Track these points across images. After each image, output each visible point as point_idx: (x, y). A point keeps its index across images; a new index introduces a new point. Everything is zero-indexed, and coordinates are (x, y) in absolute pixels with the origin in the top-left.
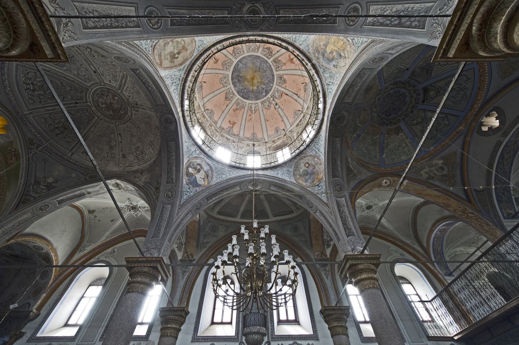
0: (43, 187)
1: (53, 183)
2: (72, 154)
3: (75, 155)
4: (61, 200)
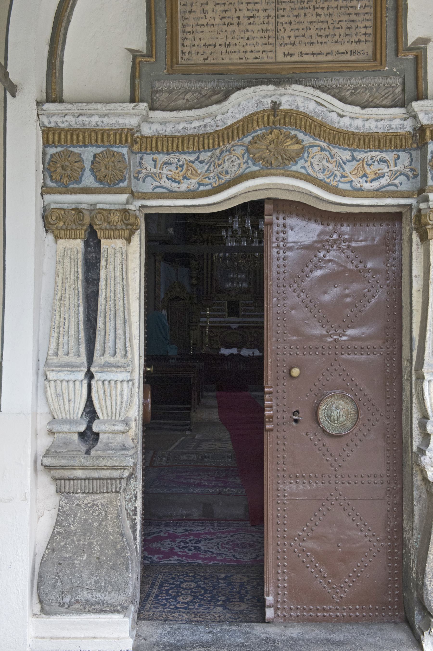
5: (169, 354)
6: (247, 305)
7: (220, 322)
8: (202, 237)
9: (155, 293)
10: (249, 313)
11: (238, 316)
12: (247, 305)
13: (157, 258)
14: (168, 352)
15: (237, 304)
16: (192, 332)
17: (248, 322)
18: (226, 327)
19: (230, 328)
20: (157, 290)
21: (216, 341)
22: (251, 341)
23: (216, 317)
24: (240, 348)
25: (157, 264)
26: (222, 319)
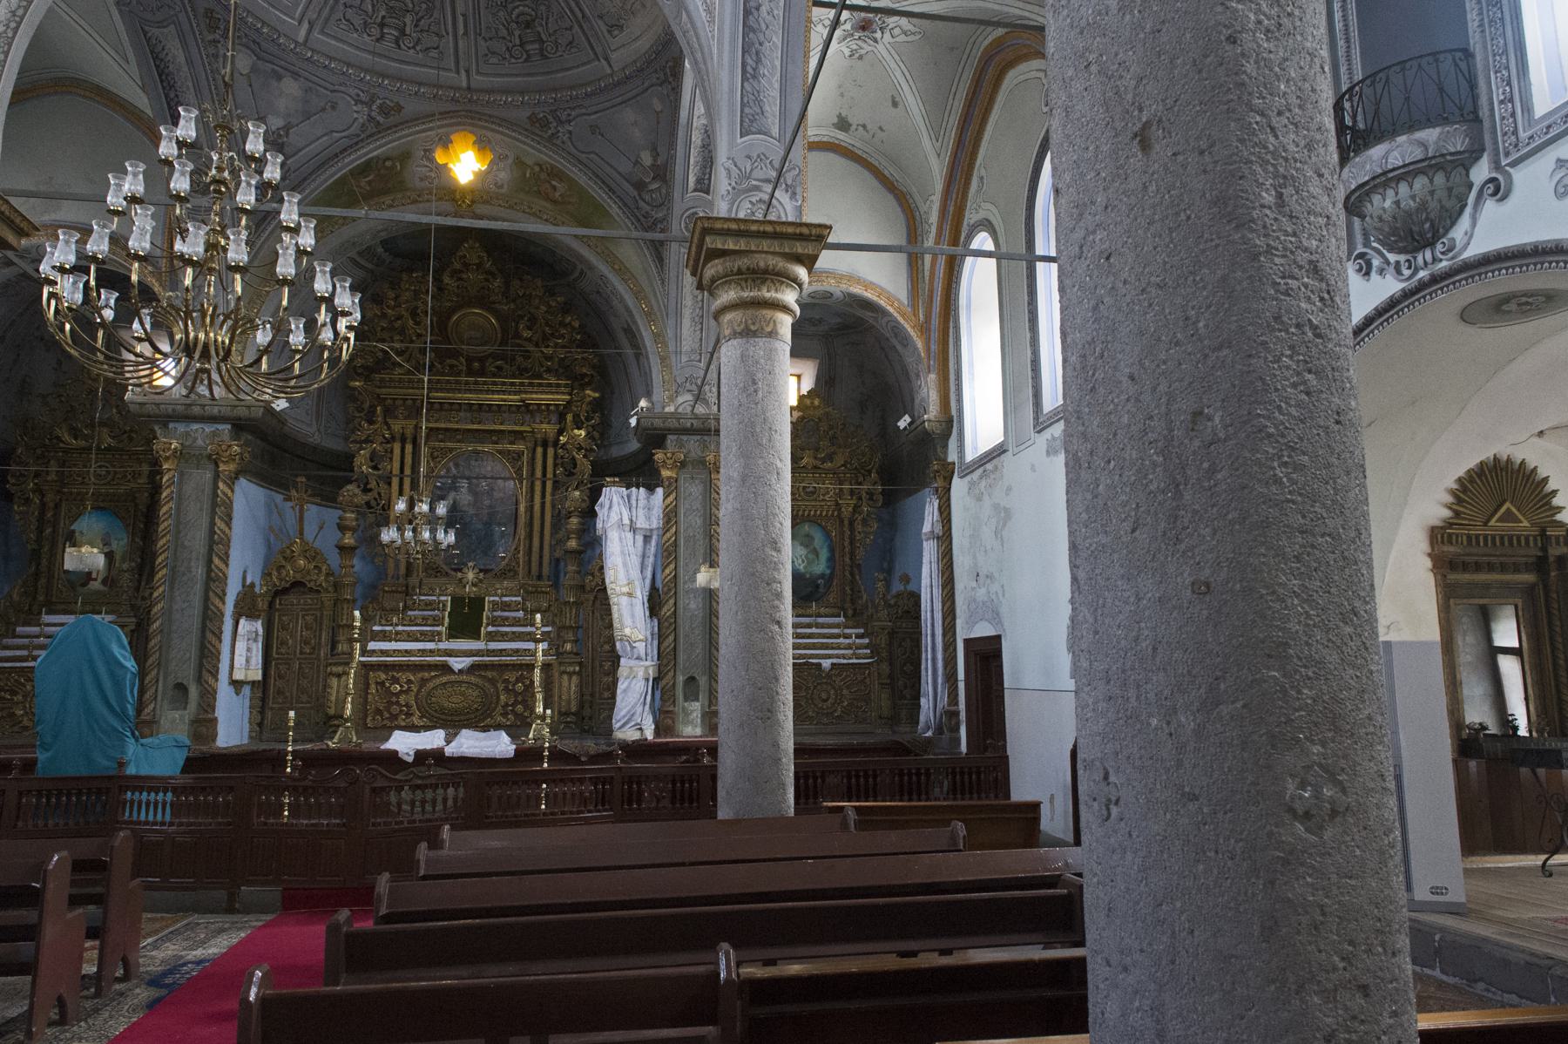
0: (654, 186)
2: (606, 59)
3: (613, 56)
4: (699, 181)
5: (131, 770)
6: (506, 607)
7: (423, 652)
8: (389, 428)
9: (209, 570)
11: (476, 635)
12: (506, 607)
13: (222, 467)
14: (121, 765)
16: (334, 682)
17: (501, 652)
19: (446, 668)
20: (216, 561)
21: (407, 705)
22: (507, 705)
23: (417, 640)
25: (221, 485)
26: (430, 646)
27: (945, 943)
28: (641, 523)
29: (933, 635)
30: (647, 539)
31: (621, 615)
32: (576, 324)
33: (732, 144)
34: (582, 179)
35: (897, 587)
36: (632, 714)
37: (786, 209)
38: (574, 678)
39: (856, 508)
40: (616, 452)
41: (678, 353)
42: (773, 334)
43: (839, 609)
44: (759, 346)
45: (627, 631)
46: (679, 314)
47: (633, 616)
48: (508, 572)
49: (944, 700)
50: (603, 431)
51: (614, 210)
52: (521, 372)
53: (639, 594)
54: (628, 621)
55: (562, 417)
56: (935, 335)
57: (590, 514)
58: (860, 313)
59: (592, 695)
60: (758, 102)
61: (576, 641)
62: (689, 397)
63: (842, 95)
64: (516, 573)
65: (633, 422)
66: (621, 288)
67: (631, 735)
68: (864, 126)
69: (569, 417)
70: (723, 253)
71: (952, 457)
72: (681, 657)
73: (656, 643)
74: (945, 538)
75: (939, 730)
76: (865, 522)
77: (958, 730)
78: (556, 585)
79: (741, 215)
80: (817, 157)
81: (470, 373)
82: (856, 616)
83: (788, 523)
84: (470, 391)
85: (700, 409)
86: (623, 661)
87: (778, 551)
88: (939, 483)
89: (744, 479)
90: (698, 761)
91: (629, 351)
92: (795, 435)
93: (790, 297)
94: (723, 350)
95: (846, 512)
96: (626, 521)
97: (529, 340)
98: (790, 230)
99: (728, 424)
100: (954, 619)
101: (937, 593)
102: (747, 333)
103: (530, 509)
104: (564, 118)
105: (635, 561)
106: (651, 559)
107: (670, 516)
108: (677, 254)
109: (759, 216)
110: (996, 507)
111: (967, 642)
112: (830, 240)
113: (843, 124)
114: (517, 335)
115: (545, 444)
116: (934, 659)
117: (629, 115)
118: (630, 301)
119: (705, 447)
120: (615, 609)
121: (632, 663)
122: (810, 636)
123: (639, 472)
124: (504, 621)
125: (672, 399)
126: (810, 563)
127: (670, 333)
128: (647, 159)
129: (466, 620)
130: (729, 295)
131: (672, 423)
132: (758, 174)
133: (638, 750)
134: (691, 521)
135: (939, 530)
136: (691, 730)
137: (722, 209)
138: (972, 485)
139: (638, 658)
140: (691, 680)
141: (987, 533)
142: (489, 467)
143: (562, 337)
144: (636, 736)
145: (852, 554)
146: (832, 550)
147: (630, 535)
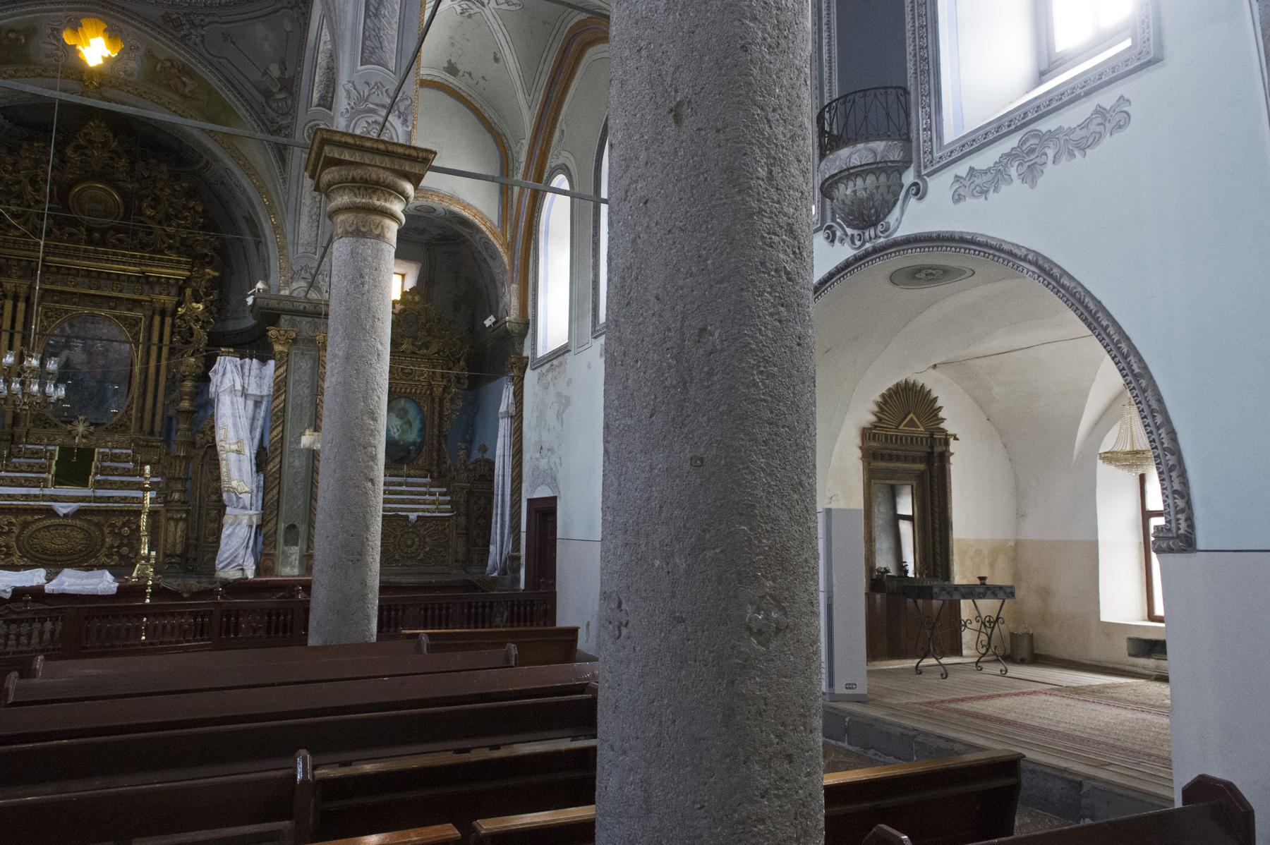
0: (281, 96)
1: (283, 73)
4: (322, 98)
6: (115, 458)
10: (117, 478)
12: (115, 458)
15: (86, 455)
17: (108, 499)
18: (40, 510)
22: (112, 547)
24: (54, 564)
27: (344, 756)
28: (253, 390)
29: (503, 495)
30: (257, 404)
31: (229, 471)
32: (200, 209)
33: (353, 67)
34: (213, 81)
35: (476, 455)
36: (236, 555)
37: (397, 132)
38: (181, 525)
39: (446, 389)
40: (233, 326)
41: (295, 244)
42: (381, 237)
43: (428, 471)
44: (368, 246)
45: (234, 484)
46: (297, 212)
47: (240, 470)
48: (121, 427)
49: (508, 547)
50: (221, 304)
51: (242, 112)
52: (143, 247)
53: (247, 451)
54: (235, 474)
55: (181, 290)
56: (519, 253)
57: (204, 379)
58: (458, 228)
59: (197, 539)
60: (378, 37)
61: (184, 491)
62: (303, 284)
63: (453, 44)
64: (128, 428)
65: (250, 300)
66: (245, 182)
67: (232, 574)
68: (470, 74)
69: (188, 291)
70: (339, 162)
71: (527, 352)
72: (284, 507)
73: (261, 495)
74: (517, 418)
75: (504, 572)
76: (452, 400)
77: (519, 570)
78: (168, 440)
79: (358, 132)
80: (426, 93)
81: (90, 242)
82: (440, 477)
83: (385, 398)
84: (89, 259)
85: (313, 295)
86: (228, 510)
87: (375, 420)
88: (515, 372)
89: (348, 358)
90: (293, 596)
91: (249, 238)
92: (395, 324)
93: (397, 207)
94: (336, 245)
95: (438, 391)
96: (238, 387)
97: (152, 218)
98: (401, 150)
99: (336, 310)
100: (521, 483)
101: (508, 461)
102: (358, 233)
103: (145, 371)
104: (197, 22)
105: (245, 423)
106: (260, 422)
107: (280, 385)
108: (298, 158)
109: (374, 135)
110: (559, 395)
111: (530, 501)
112: (435, 163)
113: (452, 69)
114: (141, 213)
115: (163, 313)
116: (503, 515)
117: (260, 30)
118: (252, 194)
119: (316, 327)
120: (223, 464)
121: (237, 511)
122: (401, 493)
123: (253, 344)
124: (114, 471)
125: (287, 284)
126: (404, 432)
127: (289, 226)
128: (275, 71)
129: (74, 468)
130: (342, 199)
131: (288, 306)
132: (374, 99)
133: (239, 587)
134: (299, 391)
135: (512, 410)
136: (289, 570)
137: (341, 124)
138: (541, 376)
139: (244, 508)
140: (292, 528)
141: (550, 414)
142: (105, 330)
143: (185, 218)
144: (237, 575)
145: (440, 425)
146: (423, 422)
147: (241, 400)
